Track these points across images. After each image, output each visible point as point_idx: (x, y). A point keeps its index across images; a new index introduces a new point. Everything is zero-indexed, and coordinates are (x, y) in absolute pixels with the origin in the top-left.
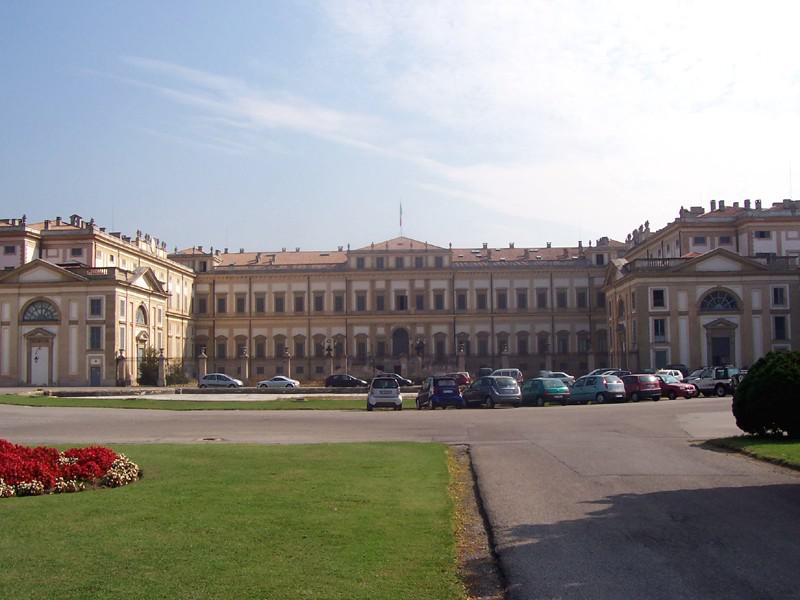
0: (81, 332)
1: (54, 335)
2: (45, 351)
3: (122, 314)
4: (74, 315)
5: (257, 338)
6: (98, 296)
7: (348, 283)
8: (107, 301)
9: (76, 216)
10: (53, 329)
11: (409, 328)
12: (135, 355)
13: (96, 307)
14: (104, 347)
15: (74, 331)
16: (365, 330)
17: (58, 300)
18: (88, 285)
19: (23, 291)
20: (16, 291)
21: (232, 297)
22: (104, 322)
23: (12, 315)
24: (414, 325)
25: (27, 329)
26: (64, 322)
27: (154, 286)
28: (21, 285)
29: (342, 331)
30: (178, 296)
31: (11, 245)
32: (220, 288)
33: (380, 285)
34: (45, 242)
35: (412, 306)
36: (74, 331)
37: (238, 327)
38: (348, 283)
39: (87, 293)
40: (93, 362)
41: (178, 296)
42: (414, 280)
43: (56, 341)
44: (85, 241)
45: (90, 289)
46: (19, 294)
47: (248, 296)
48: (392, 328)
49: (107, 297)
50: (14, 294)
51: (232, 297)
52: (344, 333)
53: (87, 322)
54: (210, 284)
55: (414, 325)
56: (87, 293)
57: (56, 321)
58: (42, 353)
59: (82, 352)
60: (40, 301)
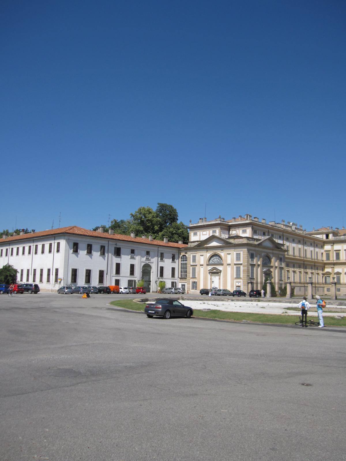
0: (232, 269)
1: (220, 271)
2: (218, 277)
4: (229, 262)
10: (220, 268)
12: (259, 280)
14: (242, 276)
22: (241, 264)
23: (204, 261)
25: (210, 268)
26: (225, 264)
30: (311, 251)
40: (237, 284)
41: (311, 251)
43: (222, 273)
53: (235, 265)
57: (222, 265)
58: (216, 279)
59: (232, 279)
60: (215, 255)
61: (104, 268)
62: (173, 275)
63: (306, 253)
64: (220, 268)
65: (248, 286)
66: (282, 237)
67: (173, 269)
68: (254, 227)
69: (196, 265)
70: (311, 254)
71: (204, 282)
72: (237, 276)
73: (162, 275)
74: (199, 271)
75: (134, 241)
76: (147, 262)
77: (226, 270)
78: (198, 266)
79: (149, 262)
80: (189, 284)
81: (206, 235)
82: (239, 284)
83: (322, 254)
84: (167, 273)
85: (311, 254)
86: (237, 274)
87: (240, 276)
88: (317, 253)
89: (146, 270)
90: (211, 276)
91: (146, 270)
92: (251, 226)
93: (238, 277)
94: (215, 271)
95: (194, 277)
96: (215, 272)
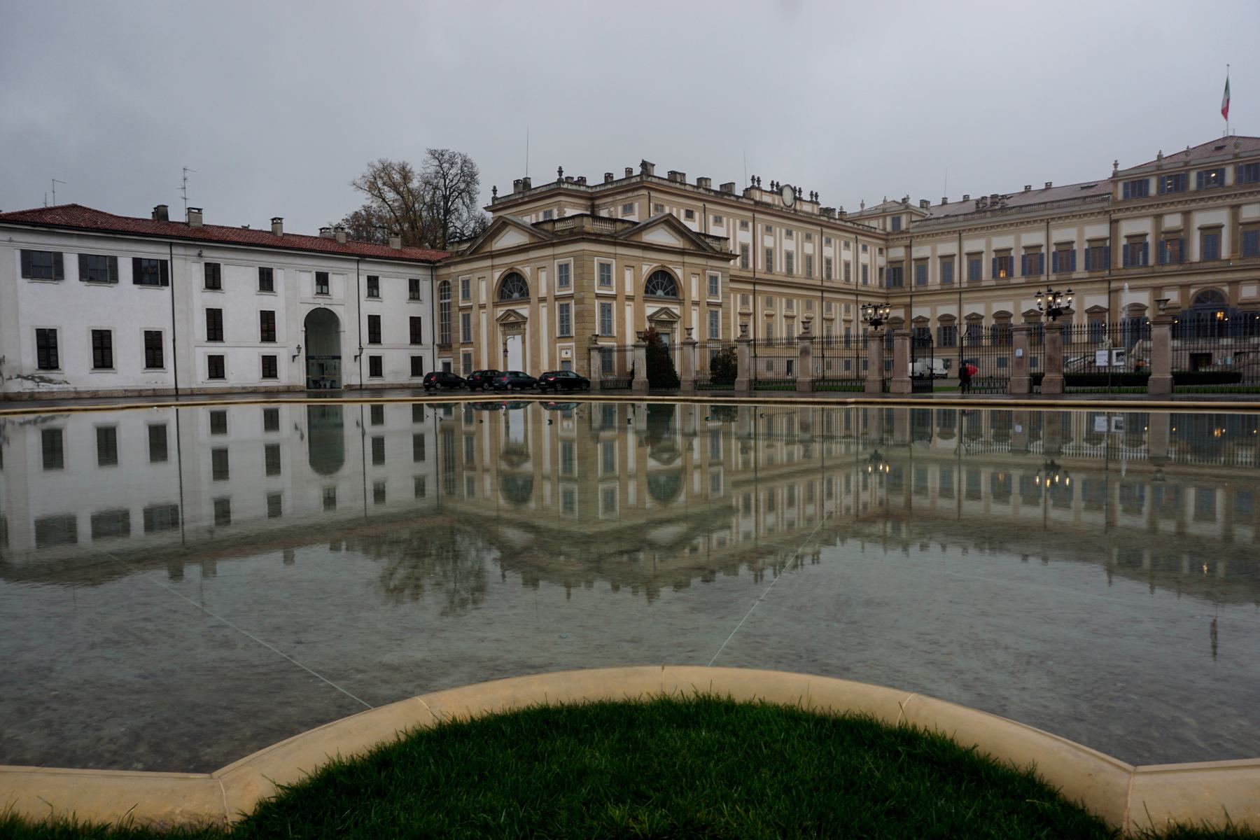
2: (519, 338)
3: (606, 280)
4: (543, 292)
5: (969, 318)
6: (563, 261)
7: (1114, 223)
10: (524, 311)
11: (1226, 289)
14: (573, 333)
15: (544, 312)
16: (1144, 298)
19: (498, 261)
20: (488, 263)
21: (934, 265)
22: (571, 297)
24: (1235, 283)
27: (693, 242)
29: (1102, 301)
30: (847, 265)
32: (918, 252)
33: (1173, 221)
35: (1234, 251)
36: (544, 312)
37: (946, 302)
38: (1114, 223)
40: (564, 355)
41: (847, 265)
42: (1239, 206)
43: (527, 326)
47: (956, 259)
48: (1193, 291)
51: (934, 265)
52: (1105, 304)
53: (557, 298)
54: (906, 247)
55: (1235, 283)
56: (554, 257)
58: (515, 344)
59: (553, 341)
61: (161, 323)
62: (416, 337)
63: (829, 269)
64: (524, 311)
65: (589, 359)
66: (750, 225)
67: (415, 323)
68: (652, 194)
69: (470, 308)
70: (847, 272)
71: (489, 353)
72: (562, 332)
73: (375, 337)
74: (478, 325)
75: (236, 239)
76: (322, 302)
77: (535, 314)
78: (475, 308)
79: (328, 301)
80: (457, 360)
82: (569, 356)
83: (881, 269)
84: (395, 330)
85: (847, 272)
86: (562, 327)
87: (568, 331)
88: (865, 267)
89: (321, 325)
90: (505, 334)
91: (321, 325)
92: (645, 192)
93: (565, 334)
94: (512, 319)
95: (467, 342)
96: (512, 325)
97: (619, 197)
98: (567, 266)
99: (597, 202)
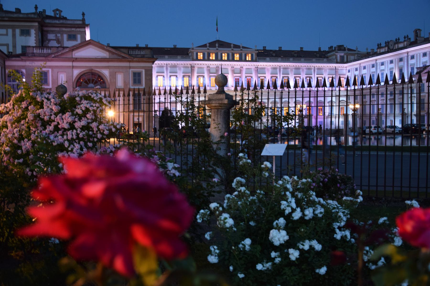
8: (145, 74)
9: (57, 10)
13: (137, 77)
17: (106, 73)
18: (130, 62)
19: (75, 64)
20: (70, 64)
28: (76, 60)
31: (27, 29)
34: (45, 29)
39: (130, 67)
44: (78, 30)
45: (132, 64)
46: (73, 67)
49: (146, 71)
50: (70, 66)
56: (130, 67)
81: (7, 35)
97: (64, 29)
98: (139, 74)
99: (45, 29)
